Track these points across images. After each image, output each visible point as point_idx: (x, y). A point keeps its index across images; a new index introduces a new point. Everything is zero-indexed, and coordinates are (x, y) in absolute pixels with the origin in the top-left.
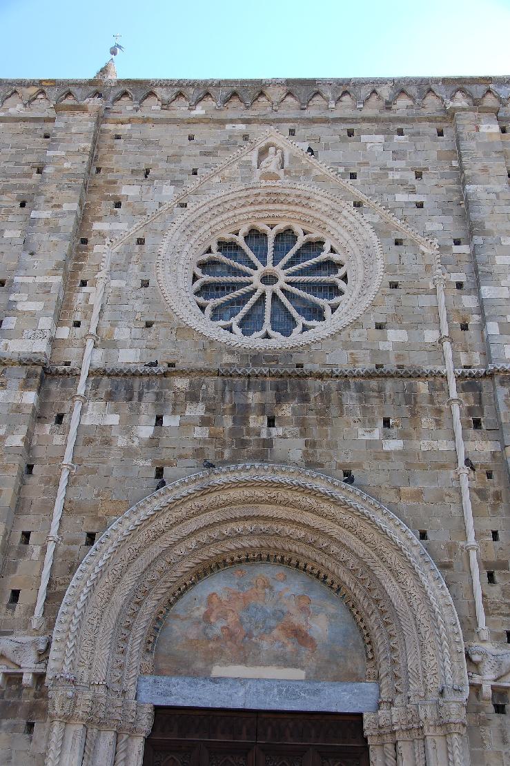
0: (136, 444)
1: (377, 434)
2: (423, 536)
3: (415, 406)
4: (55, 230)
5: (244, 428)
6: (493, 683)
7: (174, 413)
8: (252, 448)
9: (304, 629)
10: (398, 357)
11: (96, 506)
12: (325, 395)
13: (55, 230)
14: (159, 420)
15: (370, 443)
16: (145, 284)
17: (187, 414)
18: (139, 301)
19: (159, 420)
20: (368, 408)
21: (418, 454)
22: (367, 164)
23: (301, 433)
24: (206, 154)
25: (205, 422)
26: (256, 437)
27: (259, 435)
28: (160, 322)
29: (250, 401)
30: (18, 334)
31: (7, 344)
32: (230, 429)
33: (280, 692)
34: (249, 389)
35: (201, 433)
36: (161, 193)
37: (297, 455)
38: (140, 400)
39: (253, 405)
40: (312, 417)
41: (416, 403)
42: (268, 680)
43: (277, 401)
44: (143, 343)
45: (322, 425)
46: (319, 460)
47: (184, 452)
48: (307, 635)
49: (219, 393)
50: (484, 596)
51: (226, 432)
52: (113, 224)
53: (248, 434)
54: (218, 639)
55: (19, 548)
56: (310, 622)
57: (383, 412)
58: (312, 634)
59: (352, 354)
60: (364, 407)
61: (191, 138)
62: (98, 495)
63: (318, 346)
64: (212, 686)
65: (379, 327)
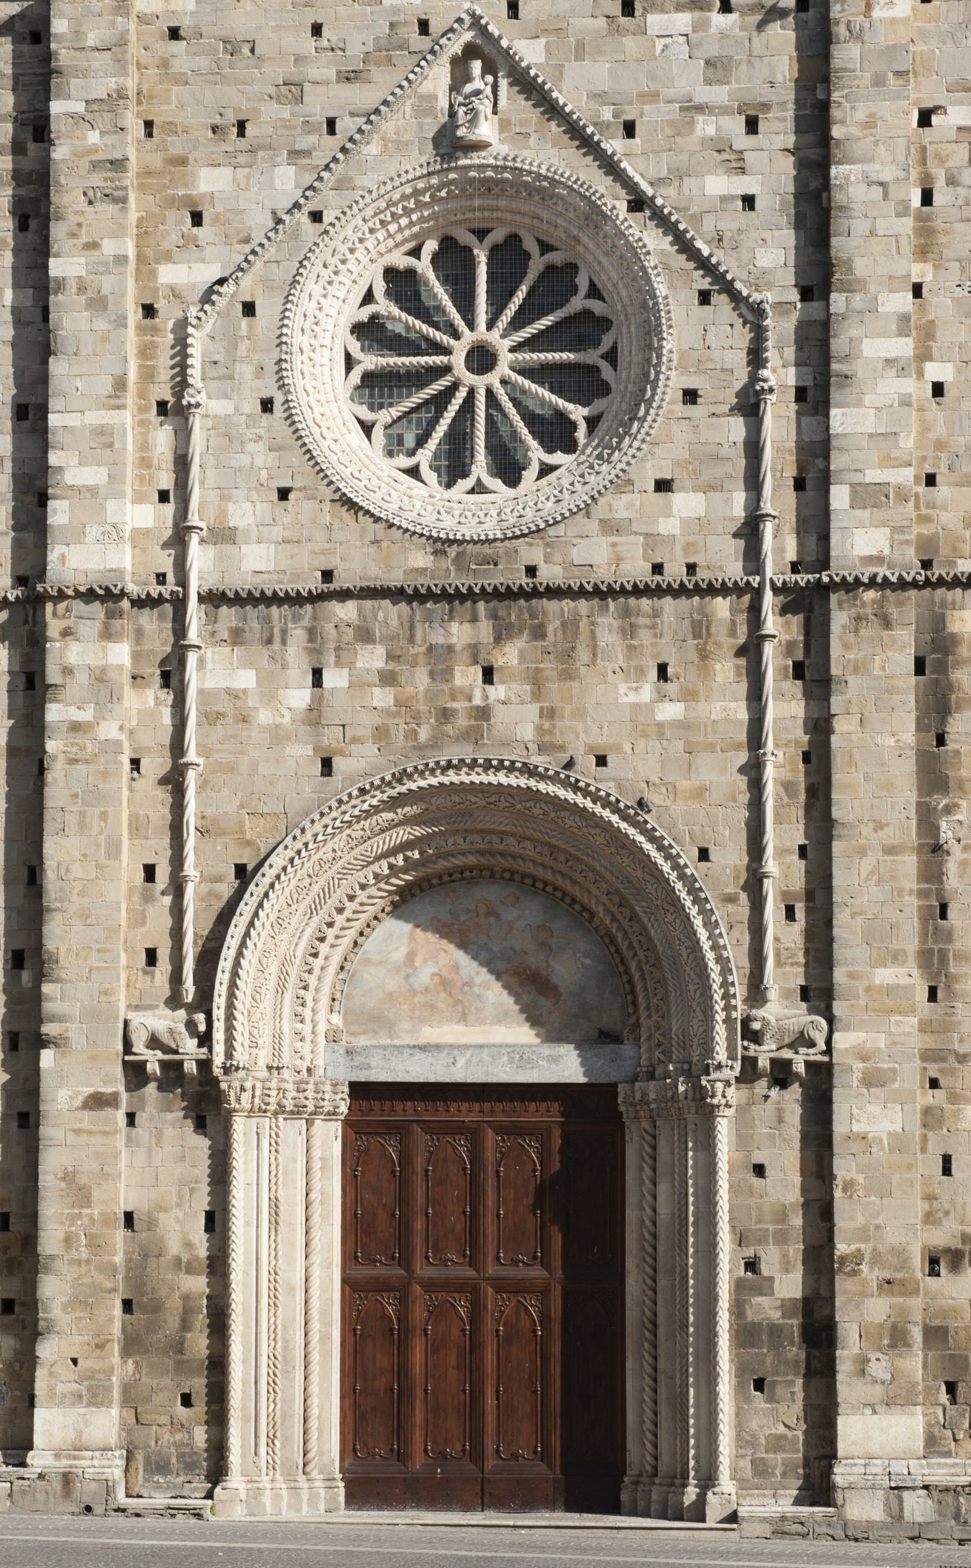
0: (287, 720)
1: (646, 692)
2: (704, 855)
3: (706, 643)
4: (98, 304)
5: (446, 687)
6: (772, 1055)
7: (338, 664)
8: (462, 722)
9: (545, 973)
10: (689, 547)
11: (242, 823)
12: (570, 626)
13: (98, 304)
14: (317, 675)
15: (636, 707)
16: (267, 405)
17: (359, 665)
18: (261, 447)
19: (317, 675)
20: (635, 647)
21: (705, 726)
22: (654, 96)
23: (533, 693)
24: (348, 77)
25: (388, 679)
26: (466, 704)
27: (470, 701)
28: (300, 490)
29: (454, 640)
30: (77, 535)
31: (63, 555)
32: (427, 691)
33: (511, 1061)
34: (451, 618)
35: (383, 697)
36: (271, 186)
37: (527, 732)
38: (284, 642)
39: (459, 648)
40: (550, 666)
41: (709, 634)
42: (494, 1046)
43: (495, 639)
44: (277, 532)
45: (565, 680)
46: (559, 739)
47: (360, 732)
48: (548, 981)
49: (406, 625)
50: (777, 939)
51: (421, 695)
52: (192, 265)
53: (453, 698)
54: (427, 990)
55: (144, 889)
56: (552, 963)
57: (658, 655)
58: (555, 979)
59: (614, 545)
60: (631, 648)
61: (317, 30)
62: (242, 806)
63: (560, 530)
64: (423, 1056)
65: (663, 486)
